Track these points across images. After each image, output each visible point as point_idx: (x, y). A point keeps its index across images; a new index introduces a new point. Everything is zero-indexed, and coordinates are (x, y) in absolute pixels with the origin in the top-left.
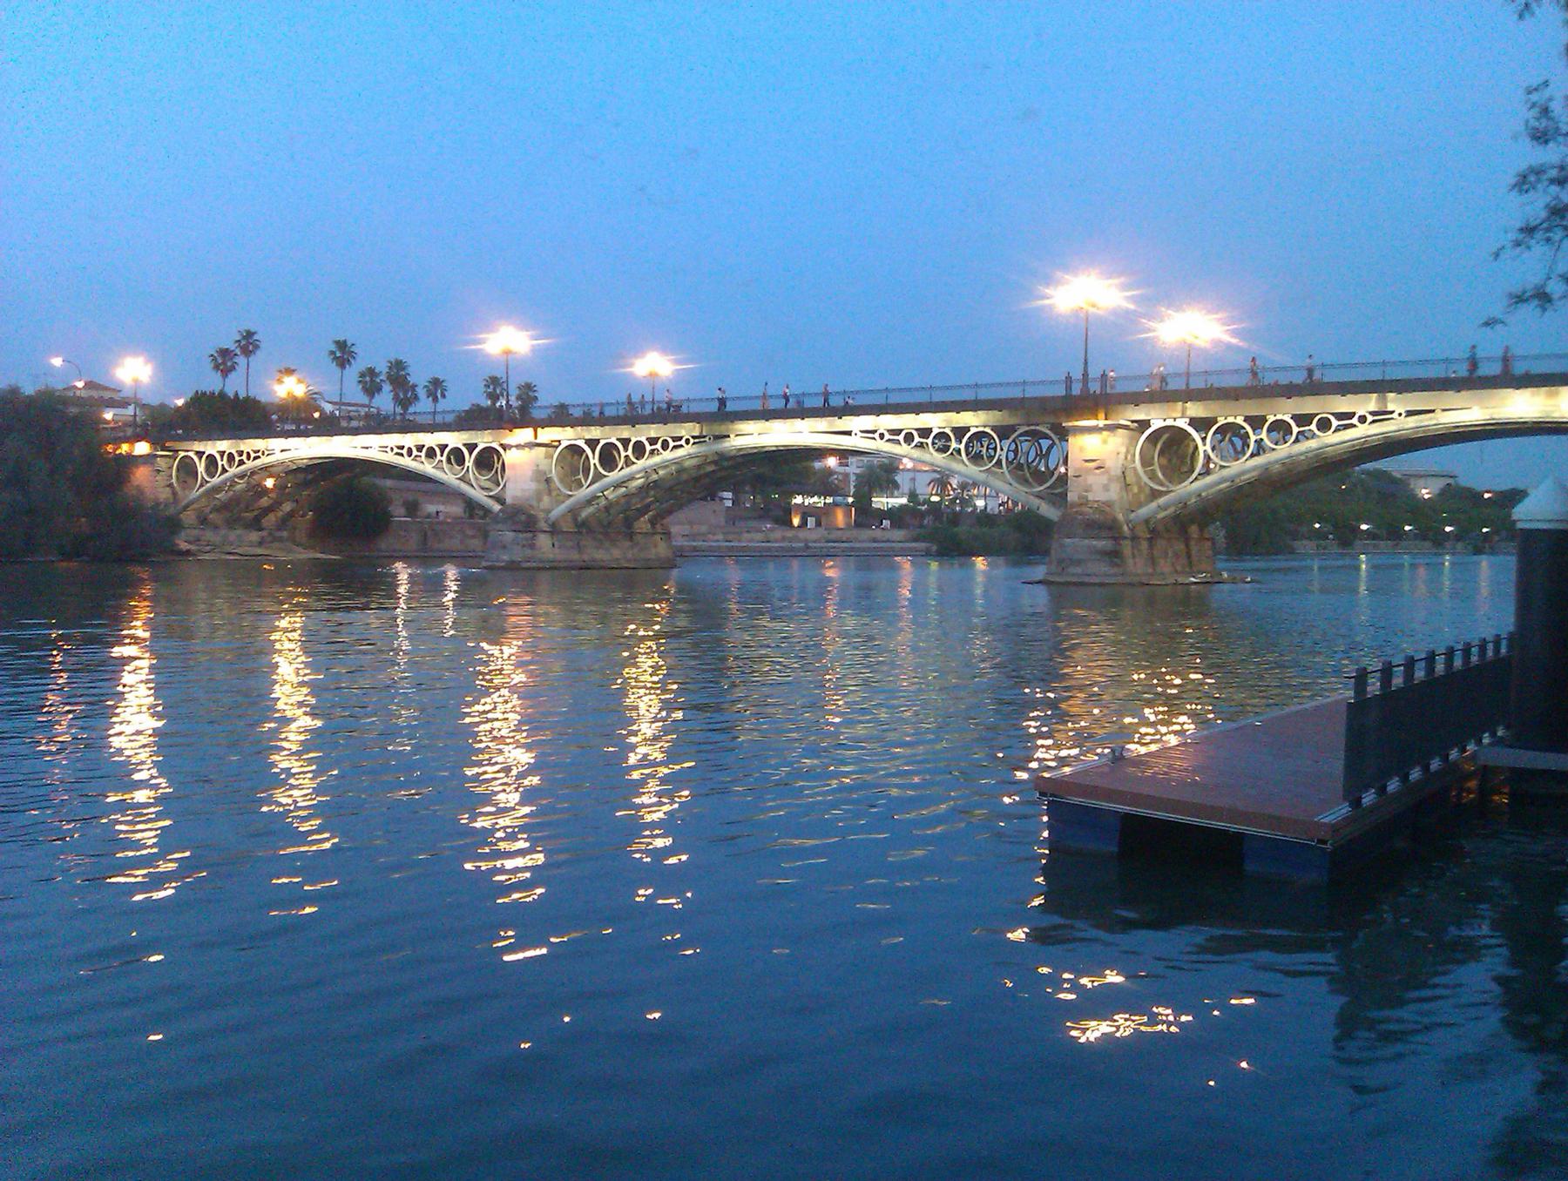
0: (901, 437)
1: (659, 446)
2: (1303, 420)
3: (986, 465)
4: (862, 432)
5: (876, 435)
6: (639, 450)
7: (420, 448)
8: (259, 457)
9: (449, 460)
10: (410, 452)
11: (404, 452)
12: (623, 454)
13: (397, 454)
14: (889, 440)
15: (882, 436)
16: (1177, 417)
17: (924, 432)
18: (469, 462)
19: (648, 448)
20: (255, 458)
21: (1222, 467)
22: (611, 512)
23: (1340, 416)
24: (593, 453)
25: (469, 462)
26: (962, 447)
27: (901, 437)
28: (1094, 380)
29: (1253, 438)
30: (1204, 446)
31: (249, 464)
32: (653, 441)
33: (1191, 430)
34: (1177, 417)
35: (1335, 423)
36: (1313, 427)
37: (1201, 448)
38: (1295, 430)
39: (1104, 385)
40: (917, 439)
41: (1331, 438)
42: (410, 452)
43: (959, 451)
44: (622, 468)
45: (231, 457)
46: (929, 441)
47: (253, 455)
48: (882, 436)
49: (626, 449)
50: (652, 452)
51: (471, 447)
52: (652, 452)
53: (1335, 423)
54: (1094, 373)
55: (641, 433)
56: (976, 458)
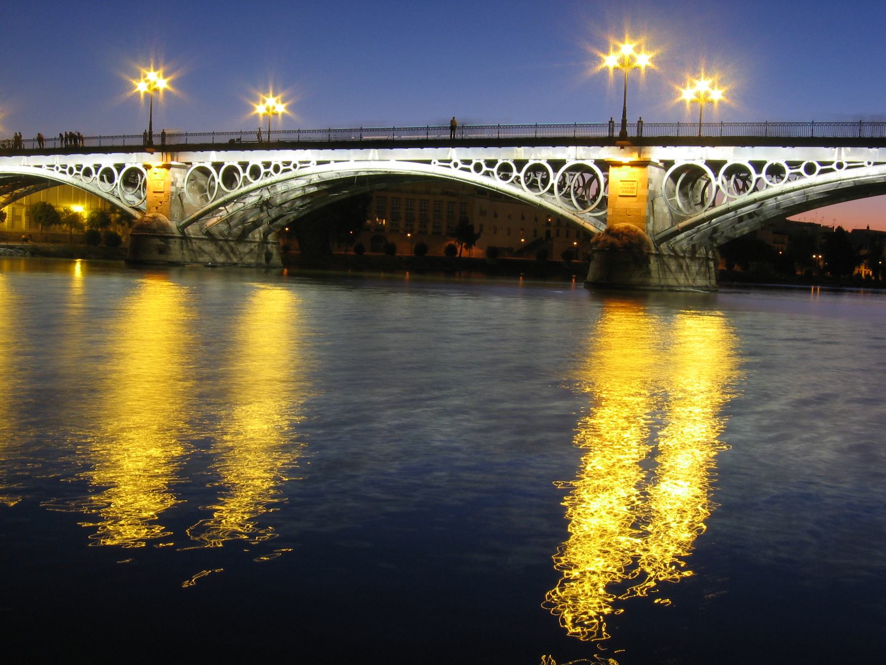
0: (471, 167)
1: (271, 169)
2: (793, 164)
3: (540, 191)
5: (451, 165)
7: (79, 168)
9: (102, 179)
10: (71, 171)
11: (67, 170)
12: (242, 175)
14: (462, 169)
16: (697, 156)
17: (491, 163)
18: (118, 179)
19: (263, 170)
22: (231, 224)
23: (822, 164)
24: (218, 174)
25: (118, 179)
26: (522, 175)
27: (471, 167)
28: (632, 125)
29: (754, 176)
32: (267, 165)
33: (707, 169)
34: (697, 156)
35: (819, 168)
38: (788, 171)
39: (640, 130)
40: (485, 168)
41: (815, 179)
42: (71, 171)
43: (518, 178)
44: (241, 187)
46: (495, 170)
49: (244, 171)
50: (267, 174)
51: (120, 167)
52: (267, 174)
54: (632, 119)
55: (256, 158)
56: (532, 186)
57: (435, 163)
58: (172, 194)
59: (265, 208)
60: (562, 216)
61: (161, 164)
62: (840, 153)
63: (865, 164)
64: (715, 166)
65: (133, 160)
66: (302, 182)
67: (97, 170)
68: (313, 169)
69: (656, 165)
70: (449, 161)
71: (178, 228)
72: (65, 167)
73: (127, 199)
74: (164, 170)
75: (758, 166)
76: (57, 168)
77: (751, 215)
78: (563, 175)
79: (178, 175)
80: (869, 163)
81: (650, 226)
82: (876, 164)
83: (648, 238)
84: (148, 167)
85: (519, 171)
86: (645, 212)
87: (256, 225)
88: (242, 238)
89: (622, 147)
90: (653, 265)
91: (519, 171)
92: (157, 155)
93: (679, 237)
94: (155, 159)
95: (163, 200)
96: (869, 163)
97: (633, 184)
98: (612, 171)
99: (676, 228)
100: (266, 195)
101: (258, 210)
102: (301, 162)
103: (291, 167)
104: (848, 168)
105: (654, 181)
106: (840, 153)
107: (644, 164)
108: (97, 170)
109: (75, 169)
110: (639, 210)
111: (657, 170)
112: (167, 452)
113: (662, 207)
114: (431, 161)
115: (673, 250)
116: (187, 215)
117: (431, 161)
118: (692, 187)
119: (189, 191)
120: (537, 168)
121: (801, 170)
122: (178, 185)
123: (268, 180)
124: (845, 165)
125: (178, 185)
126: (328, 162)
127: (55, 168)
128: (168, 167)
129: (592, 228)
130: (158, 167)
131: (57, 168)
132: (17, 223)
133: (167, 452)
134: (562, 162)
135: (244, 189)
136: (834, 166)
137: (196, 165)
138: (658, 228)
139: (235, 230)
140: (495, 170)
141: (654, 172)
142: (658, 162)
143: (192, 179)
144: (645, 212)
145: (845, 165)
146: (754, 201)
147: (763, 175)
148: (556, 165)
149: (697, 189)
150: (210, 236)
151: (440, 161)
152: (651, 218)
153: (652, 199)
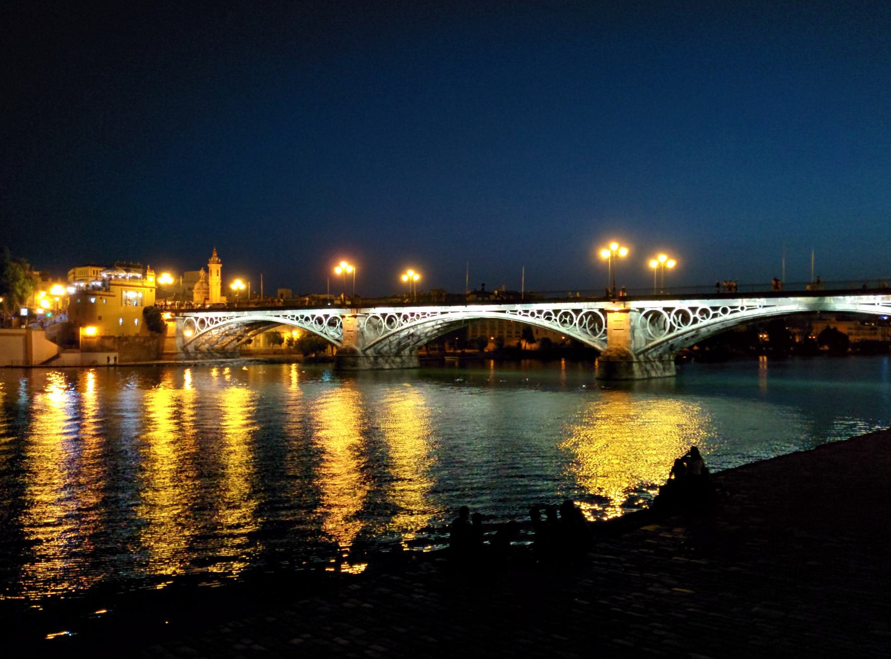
1: (415, 317)
2: (715, 309)
4: (511, 311)
5: (517, 313)
6: (405, 318)
7: (302, 317)
8: (225, 320)
9: (315, 323)
10: (297, 319)
11: (295, 318)
13: (292, 319)
14: (524, 315)
15: (520, 313)
17: (540, 312)
18: (325, 323)
20: (223, 320)
21: (678, 329)
23: (732, 307)
25: (325, 323)
26: (558, 318)
27: (529, 314)
30: (669, 319)
31: (221, 323)
32: (412, 314)
33: (663, 312)
34: (658, 305)
35: (730, 310)
36: (720, 311)
37: (668, 321)
38: (712, 313)
40: (536, 315)
41: (728, 316)
45: (212, 320)
46: (542, 315)
47: (222, 319)
48: (520, 313)
51: (326, 316)
53: (730, 310)
58: (358, 332)
59: (411, 337)
61: (351, 315)
62: (742, 301)
63: (758, 307)
64: (668, 310)
65: (333, 312)
66: (433, 323)
67: (313, 318)
68: (439, 316)
69: (634, 311)
70: (516, 311)
72: (293, 316)
73: (331, 334)
74: (353, 318)
75: (694, 309)
76: (289, 317)
77: (693, 337)
78: (582, 317)
79: (361, 321)
80: (760, 306)
81: (632, 346)
82: (764, 307)
83: (631, 353)
84: (343, 317)
85: (556, 315)
86: (629, 338)
87: (405, 347)
88: (398, 354)
89: (614, 302)
90: (635, 367)
91: (556, 315)
92: (349, 310)
93: (650, 351)
94: (347, 312)
95: (353, 335)
96: (760, 306)
98: (609, 315)
99: (647, 347)
100: (412, 331)
101: (407, 339)
102: (432, 313)
103: (426, 315)
104: (748, 309)
105: (633, 320)
106: (742, 301)
107: (627, 311)
108: (313, 318)
109: (299, 318)
110: (625, 337)
111: (635, 313)
112: (473, 474)
113: (639, 333)
115: (648, 358)
116: (367, 343)
118: (658, 320)
119: (367, 329)
120: (566, 314)
121: (720, 311)
122: (361, 326)
123: (413, 323)
124: (746, 308)
125: (361, 326)
126: (447, 313)
127: (287, 317)
128: (355, 317)
129: (599, 348)
130: (349, 317)
131: (289, 317)
132: (258, 344)
133: (473, 474)
134: (580, 311)
135: (399, 329)
136: (739, 309)
137: (371, 315)
138: (638, 346)
139: (393, 350)
140: (542, 315)
141: (634, 315)
143: (370, 322)
144: (629, 338)
145: (746, 308)
146: (693, 330)
147: (697, 315)
148: (577, 312)
149: (661, 320)
150: (379, 354)
151: (511, 311)
152: (633, 341)
153: (633, 330)
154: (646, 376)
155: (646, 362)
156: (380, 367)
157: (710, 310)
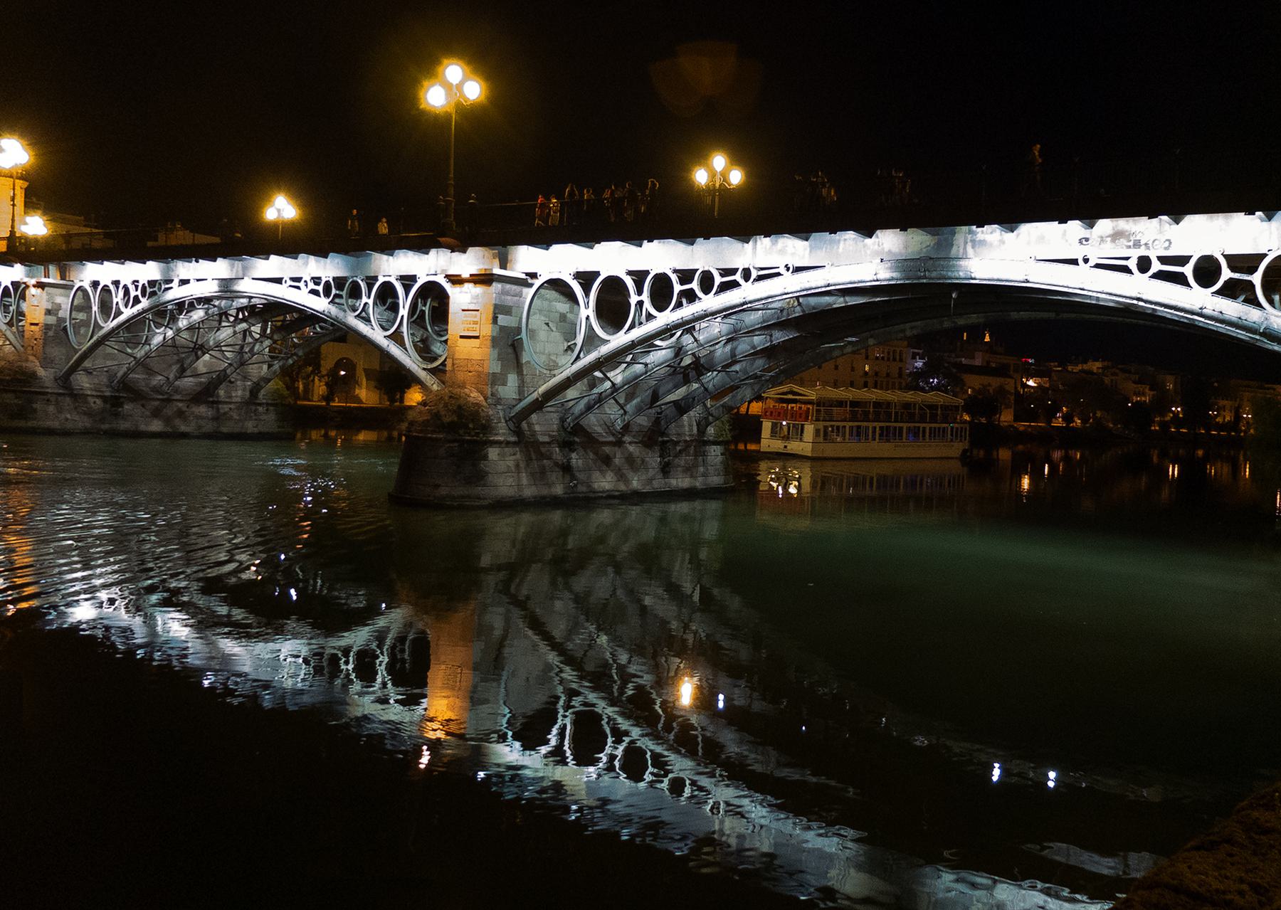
2: (686, 276)
35: (718, 280)
36: (695, 285)
57: (286, 282)
60: (409, 371)
71: (56, 380)
79: (59, 300)
82: (798, 270)
97: (476, 316)
104: (760, 278)
114: (282, 279)
117: (282, 279)
122: (61, 314)
125: (61, 314)
142: (523, 276)
145: (754, 274)
154: (559, 490)
155: (567, 446)
156: (124, 425)
157: (674, 278)
